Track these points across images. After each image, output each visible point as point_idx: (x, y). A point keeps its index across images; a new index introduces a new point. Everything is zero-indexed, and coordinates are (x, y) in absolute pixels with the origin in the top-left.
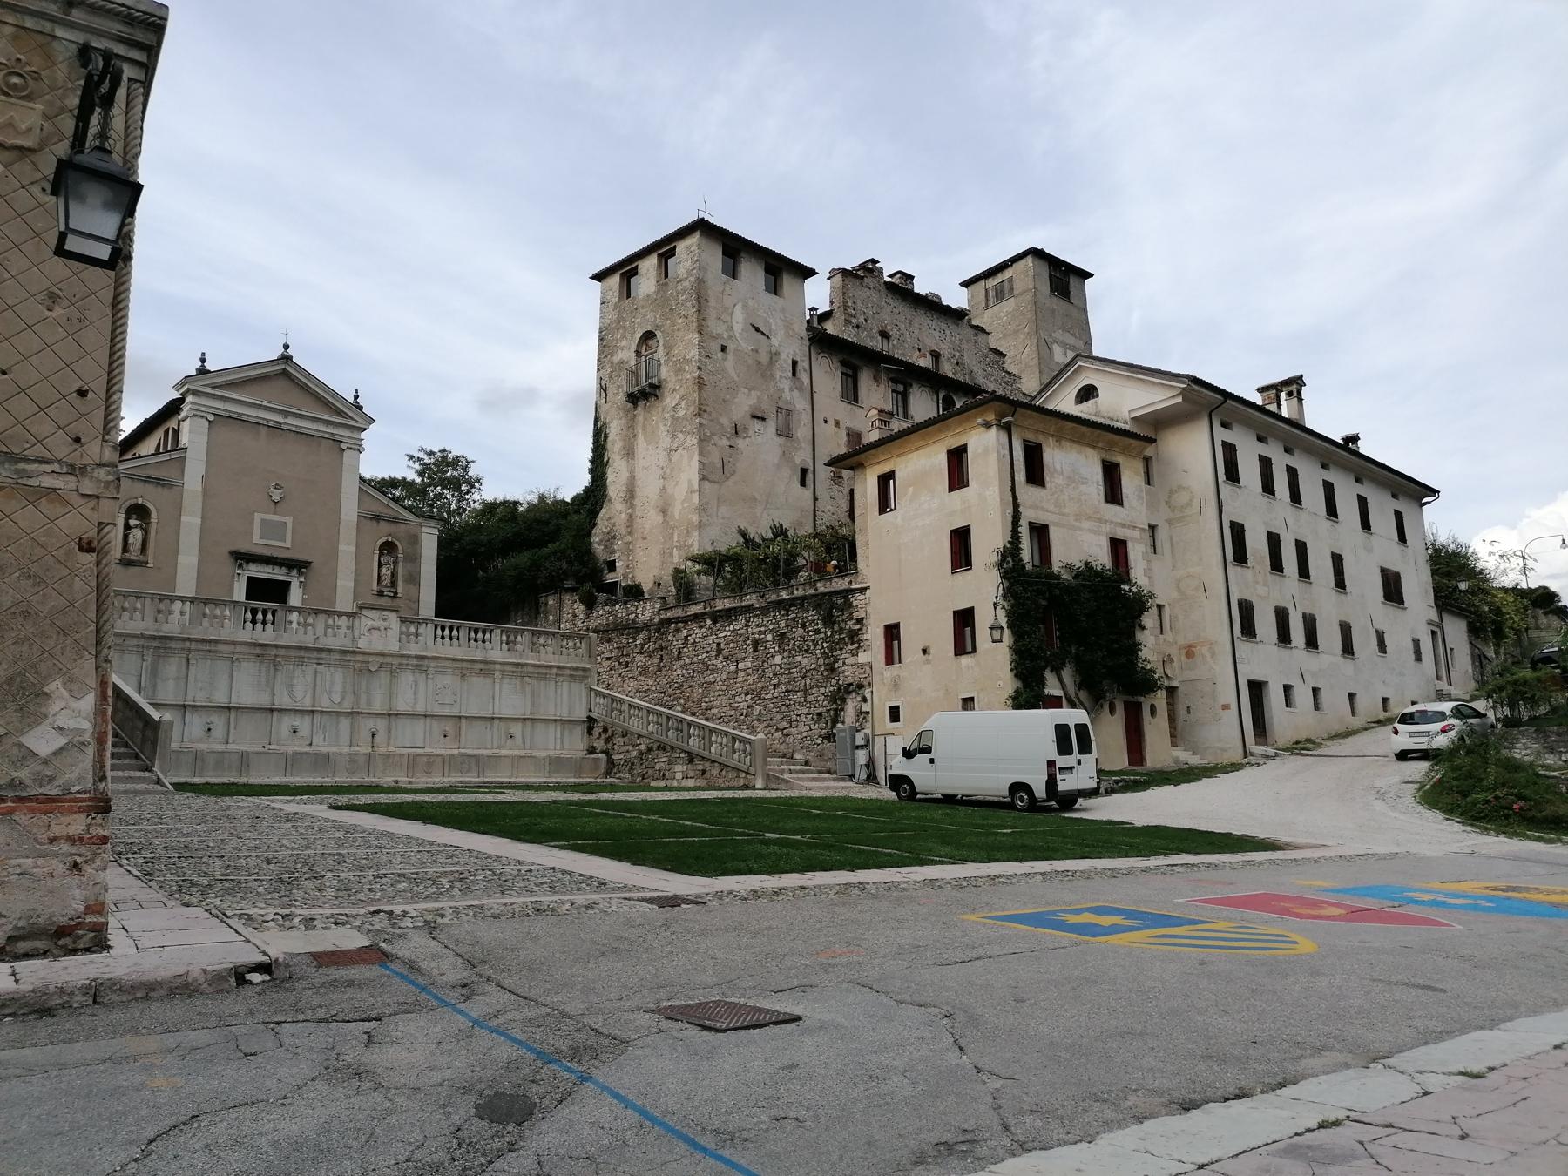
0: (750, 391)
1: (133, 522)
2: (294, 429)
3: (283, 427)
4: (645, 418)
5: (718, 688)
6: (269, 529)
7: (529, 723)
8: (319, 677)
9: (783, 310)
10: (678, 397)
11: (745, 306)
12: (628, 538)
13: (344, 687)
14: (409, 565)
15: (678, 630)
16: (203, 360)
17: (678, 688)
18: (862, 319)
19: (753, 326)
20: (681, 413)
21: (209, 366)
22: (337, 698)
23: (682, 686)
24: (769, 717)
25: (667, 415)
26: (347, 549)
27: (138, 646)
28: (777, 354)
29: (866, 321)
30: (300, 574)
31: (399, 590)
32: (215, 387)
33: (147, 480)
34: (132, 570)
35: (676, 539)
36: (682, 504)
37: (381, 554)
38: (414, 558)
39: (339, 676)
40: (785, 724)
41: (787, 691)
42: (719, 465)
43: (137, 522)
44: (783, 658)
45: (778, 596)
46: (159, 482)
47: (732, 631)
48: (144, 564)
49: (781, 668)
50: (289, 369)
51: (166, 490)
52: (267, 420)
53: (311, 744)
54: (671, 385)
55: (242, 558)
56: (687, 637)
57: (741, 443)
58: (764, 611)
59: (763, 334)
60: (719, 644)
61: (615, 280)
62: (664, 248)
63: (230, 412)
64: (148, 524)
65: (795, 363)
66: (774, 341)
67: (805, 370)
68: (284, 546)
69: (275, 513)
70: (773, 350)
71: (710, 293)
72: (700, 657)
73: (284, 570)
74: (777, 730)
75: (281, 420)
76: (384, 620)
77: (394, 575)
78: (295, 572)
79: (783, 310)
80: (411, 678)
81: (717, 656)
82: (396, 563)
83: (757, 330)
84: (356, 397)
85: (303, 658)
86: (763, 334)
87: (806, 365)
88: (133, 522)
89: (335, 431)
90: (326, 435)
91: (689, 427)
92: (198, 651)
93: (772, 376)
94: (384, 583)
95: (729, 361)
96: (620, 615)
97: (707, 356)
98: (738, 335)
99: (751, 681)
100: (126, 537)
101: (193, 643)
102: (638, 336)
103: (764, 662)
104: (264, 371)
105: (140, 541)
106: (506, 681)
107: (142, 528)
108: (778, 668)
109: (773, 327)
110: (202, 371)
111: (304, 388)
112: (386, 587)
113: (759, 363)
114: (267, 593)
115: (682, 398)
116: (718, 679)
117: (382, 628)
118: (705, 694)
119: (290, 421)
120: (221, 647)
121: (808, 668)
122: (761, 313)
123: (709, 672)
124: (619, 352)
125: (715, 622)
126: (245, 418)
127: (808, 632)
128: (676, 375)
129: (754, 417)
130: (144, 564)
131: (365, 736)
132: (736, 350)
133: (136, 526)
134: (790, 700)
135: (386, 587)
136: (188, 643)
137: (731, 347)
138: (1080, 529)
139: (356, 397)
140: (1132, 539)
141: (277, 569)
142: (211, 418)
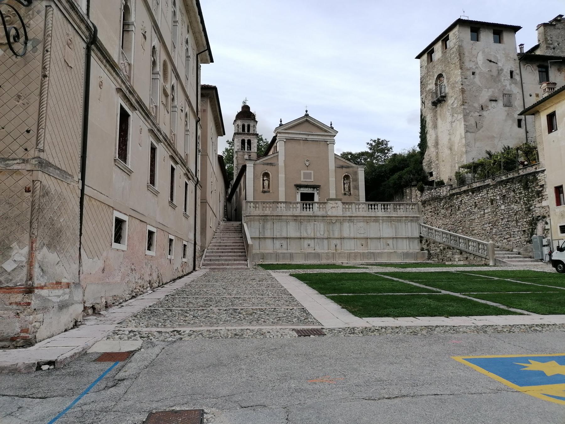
0: (488, 89)
1: (265, 178)
2: (311, 140)
3: (308, 139)
4: (440, 110)
5: (476, 221)
6: (307, 176)
7: (395, 240)
8: (315, 225)
9: (504, 49)
10: (453, 99)
11: (483, 52)
12: (437, 162)
13: (324, 229)
14: (355, 183)
15: (457, 198)
16: (281, 121)
17: (459, 222)
18: (556, 44)
19: (488, 60)
20: (455, 106)
21: (283, 123)
22: (322, 233)
23: (461, 221)
24: (500, 233)
25: (449, 108)
26: (332, 179)
27: (258, 219)
28: (502, 70)
29: (558, 44)
30: (317, 190)
31: (352, 192)
32: (285, 130)
33: (268, 164)
34: (266, 194)
35: (456, 160)
36: (458, 144)
37: (344, 180)
38: (356, 180)
39: (322, 225)
40: (508, 236)
41: (508, 221)
42: (474, 125)
43: (266, 178)
44: (505, 207)
45: (501, 179)
46: (271, 164)
47: (481, 196)
48: (269, 192)
49: (504, 211)
50: (308, 119)
51: (273, 167)
52: (302, 138)
53: (315, 250)
54: (450, 95)
55: (298, 186)
56: (461, 200)
57: (485, 113)
58: (495, 186)
59: (494, 62)
60: (475, 202)
61: (425, 57)
62: (444, 38)
63: (291, 137)
64: (269, 178)
65: (511, 73)
66: (500, 64)
67: (517, 74)
68: (311, 181)
70: (500, 68)
71: (465, 50)
72: (468, 209)
73: (312, 189)
74: (504, 239)
75: (307, 137)
76: (336, 204)
77: (349, 187)
78: (315, 190)
79: (504, 49)
80: (348, 224)
81: (475, 207)
82: (349, 183)
83: (490, 61)
84: (331, 124)
85: (310, 219)
86: (494, 62)
87: (518, 72)
88: (265, 178)
89: (325, 138)
90: (322, 140)
91: (459, 111)
92: (276, 219)
93: (500, 81)
94: (346, 190)
96: (434, 194)
97: (466, 78)
98: (480, 66)
99: (491, 218)
100: (263, 183)
101: (275, 217)
102: (435, 77)
103: (496, 209)
104: (300, 121)
105: (267, 184)
106: (384, 223)
107: (268, 180)
108: (503, 211)
109: (499, 58)
110: (281, 125)
111: (313, 125)
112: (347, 191)
113: (492, 76)
114: (307, 198)
115: (455, 99)
116: (476, 218)
117: (336, 207)
118: (471, 224)
119: (310, 137)
120: (283, 217)
121: (517, 210)
122: (492, 53)
123: (472, 215)
124: (429, 85)
125: (473, 193)
126: (295, 139)
127: (516, 194)
128: (452, 90)
129: (491, 100)
130: (269, 192)
131: (333, 246)
132: (480, 73)
133: (266, 180)
134: (510, 225)
135: (347, 191)
136: (273, 217)
137: (477, 72)
139: (331, 124)
141: (310, 189)
142: (285, 140)
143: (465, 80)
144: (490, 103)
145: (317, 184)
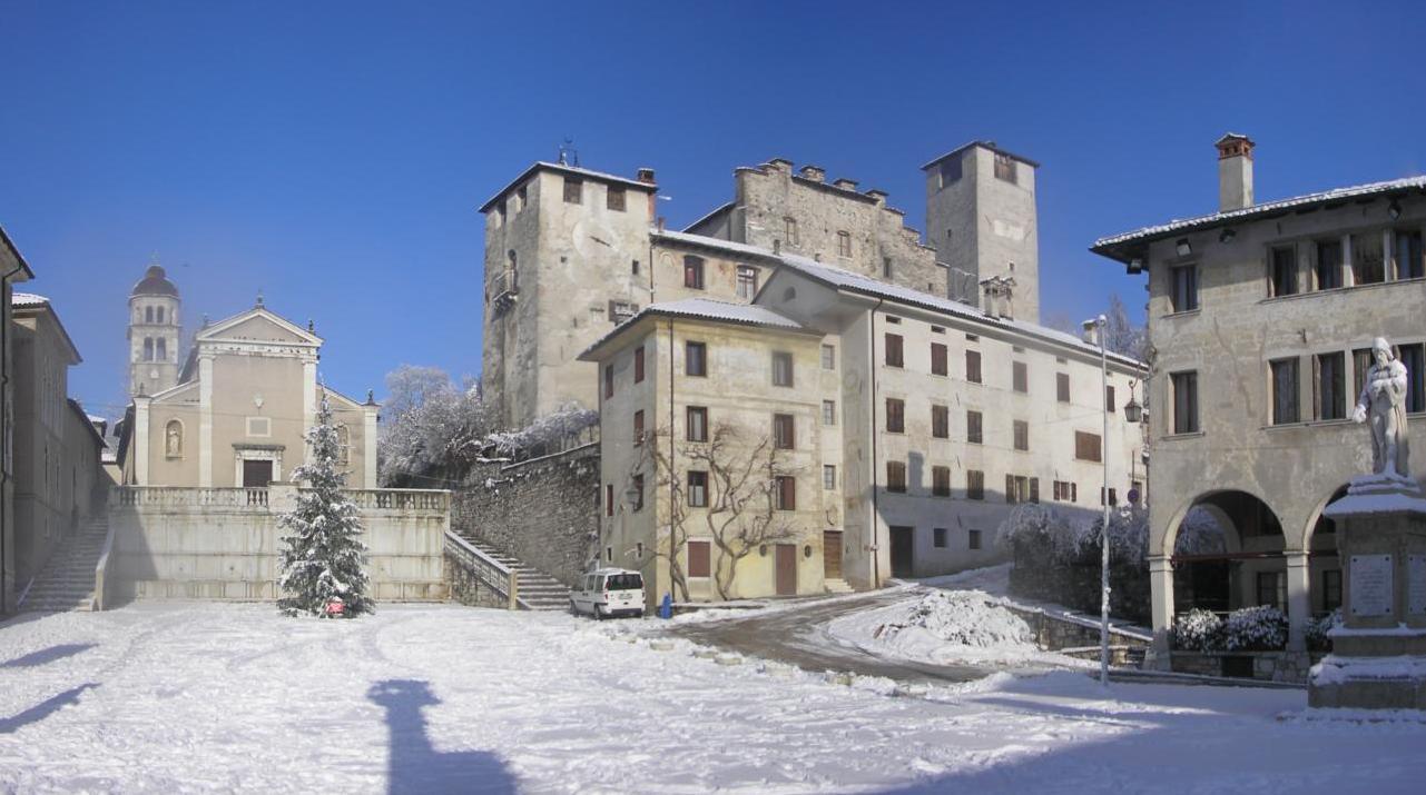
19: (593, 238)
31: (349, 460)
34: (175, 462)
55: (239, 447)
59: (603, 243)
65: (635, 264)
67: (646, 268)
68: (267, 437)
69: (259, 415)
73: (268, 453)
83: (598, 240)
86: (603, 243)
87: (648, 263)
95: (569, 268)
98: (578, 247)
100: (168, 442)
105: (176, 444)
129: (592, 310)
137: (570, 257)
138: (744, 409)
140: (800, 414)
143: (548, 271)
144: (589, 314)
145: (278, 441)
